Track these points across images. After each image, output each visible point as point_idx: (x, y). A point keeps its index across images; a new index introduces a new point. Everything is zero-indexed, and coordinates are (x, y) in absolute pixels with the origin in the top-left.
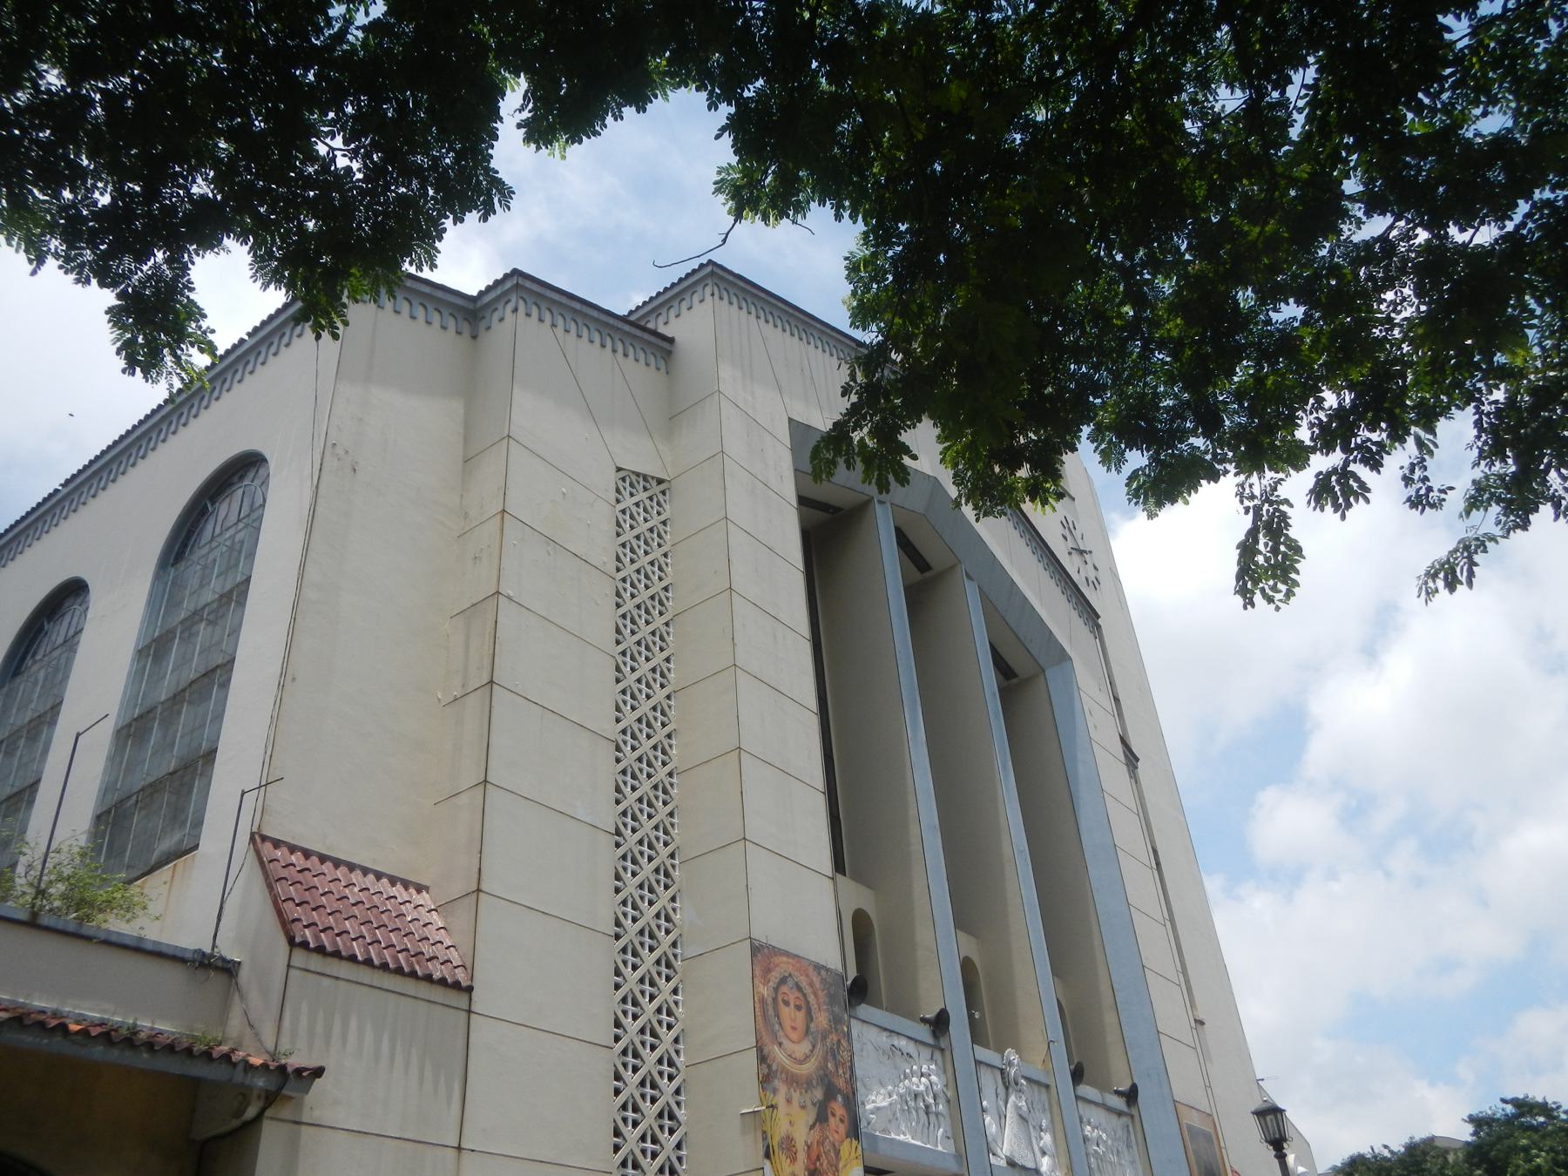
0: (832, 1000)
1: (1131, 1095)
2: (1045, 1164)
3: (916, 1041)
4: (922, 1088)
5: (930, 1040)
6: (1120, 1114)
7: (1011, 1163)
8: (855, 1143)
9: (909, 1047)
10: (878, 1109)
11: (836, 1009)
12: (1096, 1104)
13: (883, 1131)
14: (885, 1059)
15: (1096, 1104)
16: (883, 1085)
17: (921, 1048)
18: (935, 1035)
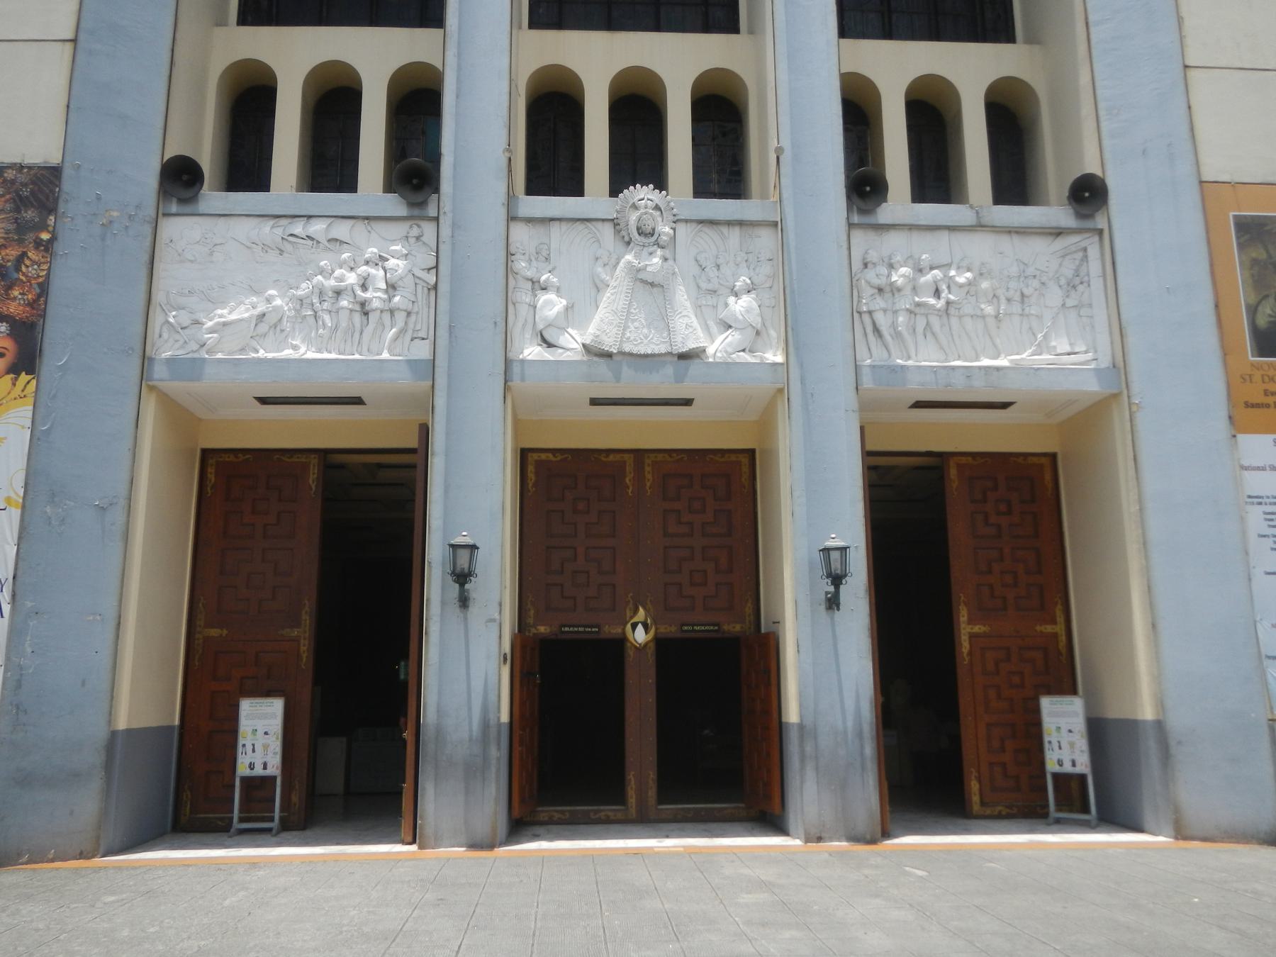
0: (20, 203)
1: (1088, 194)
2: (718, 346)
3: (367, 218)
4: (352, 278)
5: (402, 210)
6: (1058, 233)
7: (595, 352)
8: (24, 377)
9: (342, 230)
10: (225, 324)
11: (29, 214)
12: (951, 229)
13: (242, 350)
14: (273, 256)
15: (951, 229)
16: (256, 292)
17: (380, 227)
18: (411, 205)
